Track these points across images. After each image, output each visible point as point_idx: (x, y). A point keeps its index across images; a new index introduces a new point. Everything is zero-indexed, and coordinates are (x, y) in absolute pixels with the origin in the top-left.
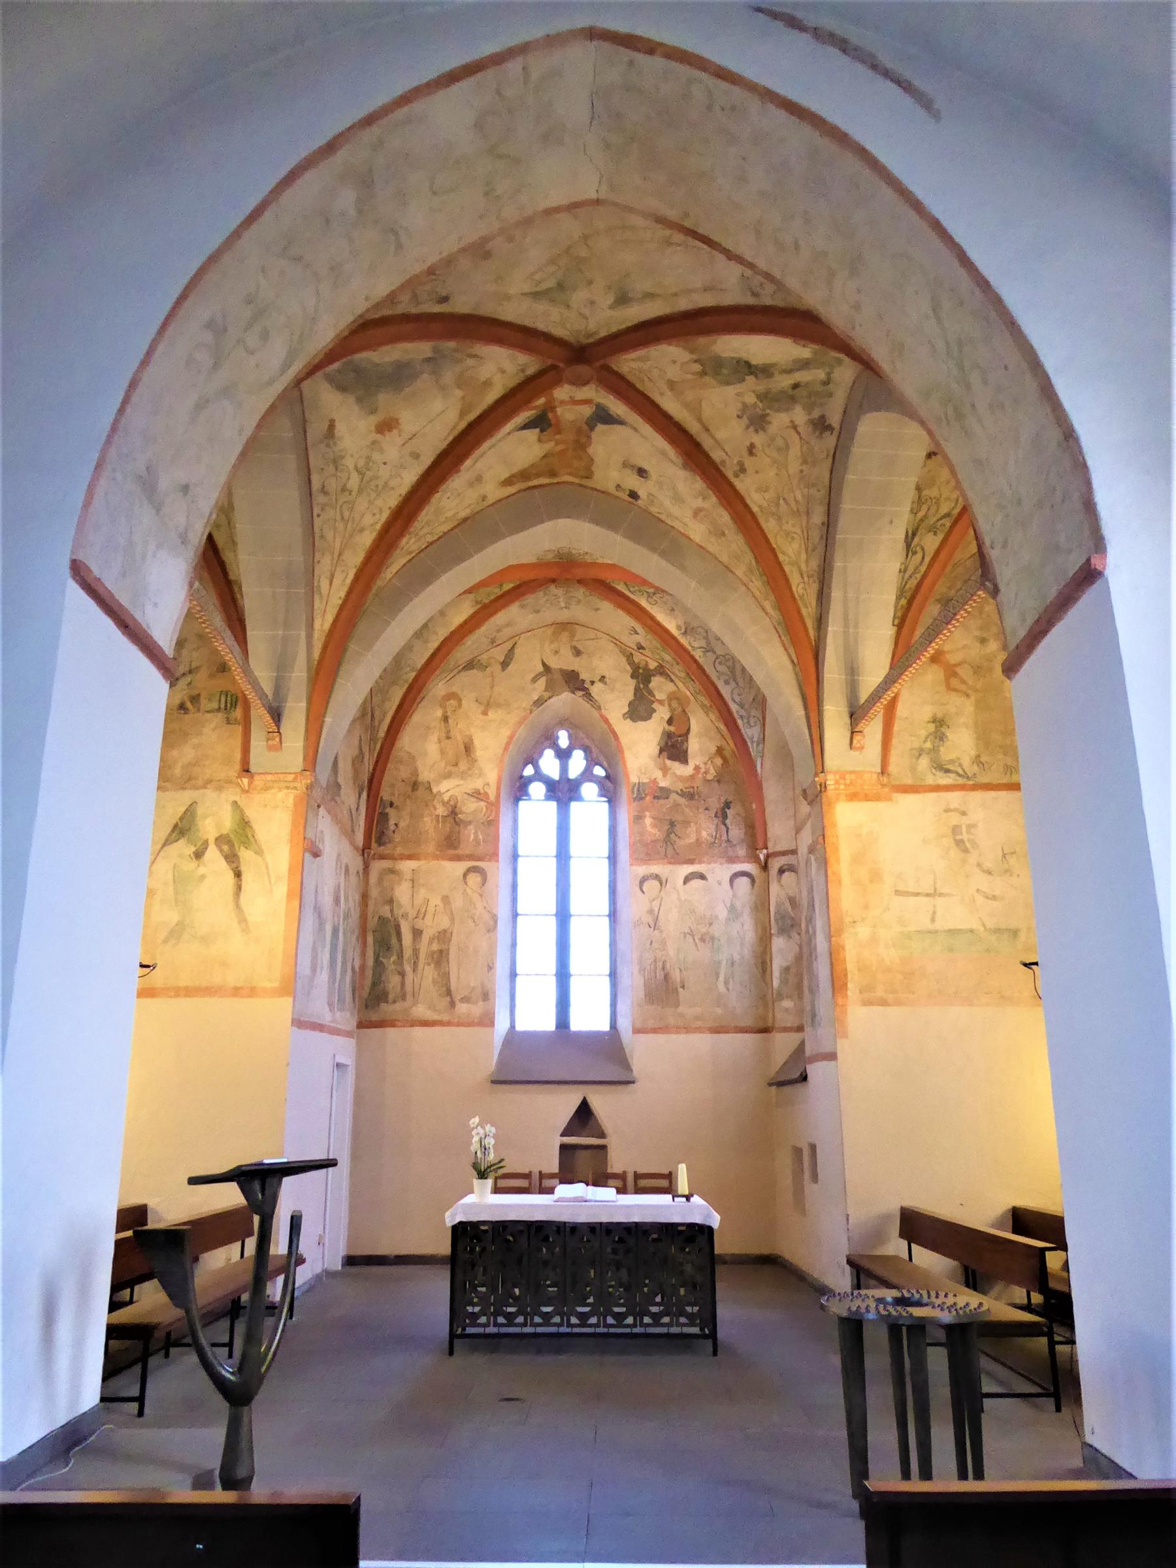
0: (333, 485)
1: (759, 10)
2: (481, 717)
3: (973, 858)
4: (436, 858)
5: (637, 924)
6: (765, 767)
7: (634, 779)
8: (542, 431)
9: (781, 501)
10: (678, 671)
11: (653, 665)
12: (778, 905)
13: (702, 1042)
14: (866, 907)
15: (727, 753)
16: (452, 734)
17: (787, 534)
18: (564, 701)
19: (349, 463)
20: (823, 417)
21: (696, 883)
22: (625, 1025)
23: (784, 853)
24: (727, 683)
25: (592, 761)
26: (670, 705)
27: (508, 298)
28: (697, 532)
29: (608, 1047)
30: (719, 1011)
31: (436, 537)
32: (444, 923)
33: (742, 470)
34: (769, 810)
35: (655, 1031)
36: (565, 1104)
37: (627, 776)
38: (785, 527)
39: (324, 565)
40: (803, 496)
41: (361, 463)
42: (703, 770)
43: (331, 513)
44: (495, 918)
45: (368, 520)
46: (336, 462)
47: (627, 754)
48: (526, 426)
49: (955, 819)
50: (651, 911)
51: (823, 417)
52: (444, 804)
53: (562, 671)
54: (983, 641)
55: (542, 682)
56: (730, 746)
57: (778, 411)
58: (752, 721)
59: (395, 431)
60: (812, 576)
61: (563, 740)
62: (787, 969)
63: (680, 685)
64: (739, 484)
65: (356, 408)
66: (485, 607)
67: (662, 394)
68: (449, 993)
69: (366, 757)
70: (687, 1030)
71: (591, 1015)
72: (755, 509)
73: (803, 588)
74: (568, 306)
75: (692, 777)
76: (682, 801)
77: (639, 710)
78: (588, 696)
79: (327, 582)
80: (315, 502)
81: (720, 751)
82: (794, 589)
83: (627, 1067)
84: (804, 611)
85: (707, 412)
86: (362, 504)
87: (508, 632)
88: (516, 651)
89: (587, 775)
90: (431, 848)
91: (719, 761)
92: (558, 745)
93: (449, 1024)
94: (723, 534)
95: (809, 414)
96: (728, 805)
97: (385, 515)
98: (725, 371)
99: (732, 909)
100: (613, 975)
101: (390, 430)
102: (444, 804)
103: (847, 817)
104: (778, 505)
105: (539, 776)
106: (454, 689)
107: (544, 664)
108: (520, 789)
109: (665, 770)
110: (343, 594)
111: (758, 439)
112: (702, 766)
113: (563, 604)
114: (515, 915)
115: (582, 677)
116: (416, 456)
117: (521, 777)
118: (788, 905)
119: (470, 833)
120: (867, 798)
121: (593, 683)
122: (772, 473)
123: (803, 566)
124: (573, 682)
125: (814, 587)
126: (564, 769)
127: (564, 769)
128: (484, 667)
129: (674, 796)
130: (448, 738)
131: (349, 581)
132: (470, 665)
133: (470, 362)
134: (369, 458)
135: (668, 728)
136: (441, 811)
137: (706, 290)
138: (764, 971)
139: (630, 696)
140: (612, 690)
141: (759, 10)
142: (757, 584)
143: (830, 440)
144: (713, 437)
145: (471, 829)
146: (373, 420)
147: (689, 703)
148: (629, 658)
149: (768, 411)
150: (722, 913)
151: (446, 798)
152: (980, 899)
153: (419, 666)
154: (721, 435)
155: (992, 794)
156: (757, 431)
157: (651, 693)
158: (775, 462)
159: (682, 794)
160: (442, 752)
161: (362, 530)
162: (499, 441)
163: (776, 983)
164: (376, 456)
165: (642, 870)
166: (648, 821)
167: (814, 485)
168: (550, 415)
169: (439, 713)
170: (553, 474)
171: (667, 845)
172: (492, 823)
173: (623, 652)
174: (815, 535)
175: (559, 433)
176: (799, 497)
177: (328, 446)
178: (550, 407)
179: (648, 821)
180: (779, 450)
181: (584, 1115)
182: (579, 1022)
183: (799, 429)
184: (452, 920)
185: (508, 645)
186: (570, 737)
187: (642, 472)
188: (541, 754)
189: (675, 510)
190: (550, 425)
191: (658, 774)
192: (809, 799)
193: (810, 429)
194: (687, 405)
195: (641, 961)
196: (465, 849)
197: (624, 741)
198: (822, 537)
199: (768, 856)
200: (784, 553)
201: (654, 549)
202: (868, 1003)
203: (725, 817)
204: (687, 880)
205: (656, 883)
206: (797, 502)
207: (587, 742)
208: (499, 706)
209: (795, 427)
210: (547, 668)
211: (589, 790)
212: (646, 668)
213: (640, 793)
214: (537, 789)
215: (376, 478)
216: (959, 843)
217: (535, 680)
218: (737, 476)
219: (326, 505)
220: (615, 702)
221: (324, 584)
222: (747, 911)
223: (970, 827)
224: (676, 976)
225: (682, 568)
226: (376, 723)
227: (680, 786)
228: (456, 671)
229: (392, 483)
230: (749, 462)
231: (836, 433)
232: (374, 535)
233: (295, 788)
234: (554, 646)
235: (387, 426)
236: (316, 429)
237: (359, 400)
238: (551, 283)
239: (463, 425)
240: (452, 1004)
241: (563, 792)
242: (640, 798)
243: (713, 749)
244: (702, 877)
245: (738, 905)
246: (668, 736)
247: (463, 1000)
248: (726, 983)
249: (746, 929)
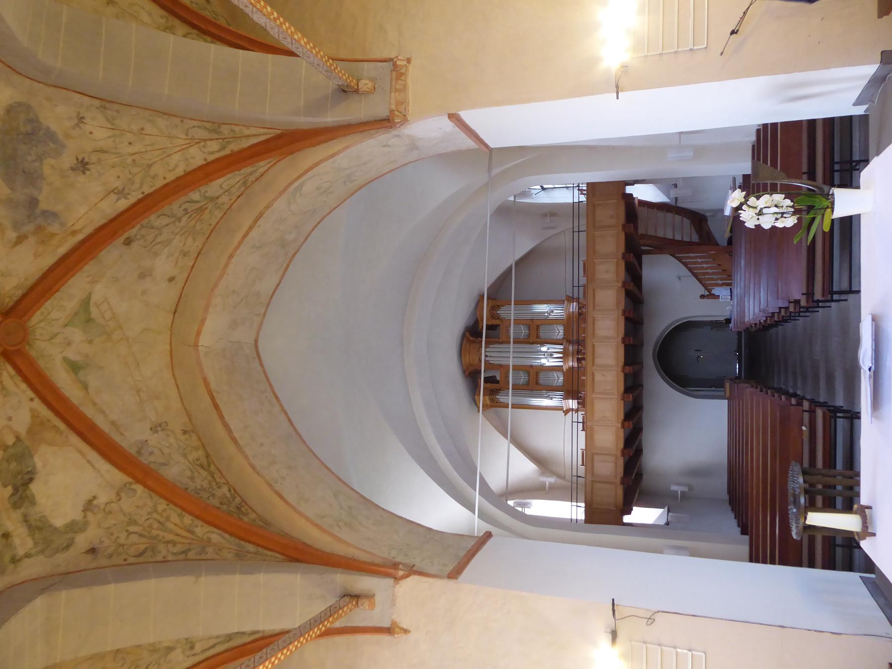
27: (93, 282)
74: (66, 326)
98: (13, 465)
133: (12, 235)
137: (113, 423)
238: (94, 312)
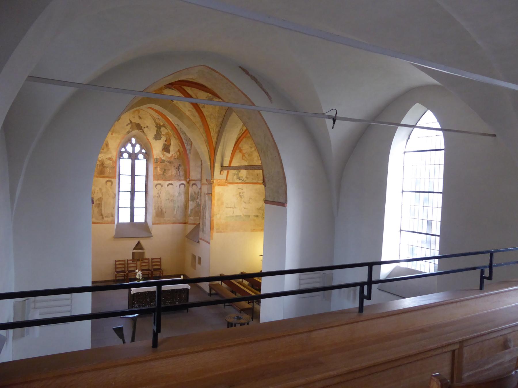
1: (240, 67)
3: (243, 200)
4: (97, 177)
5: (154, 197)
6: (191, 157)
7: (155, 157)
10: (169, 127)
11: (162, 124)
12: (191, 193)
13: (170, 227)
14: (219, 211)
15: (181, 151)
18: (136, 132)
21: (170, 186)
22: (150, 222)
23: (194, 180)
25: (142, 148)
28: (188, 113)
29: (144, 226)
30: (174, 219)
32: (100, 196)
33: (204, 107)
34: (191, 168)
35: (158, 224)
36: (133, 243)
37: (153, 156)
44: (115, 194)
47: (154, 150)
49: (240, 191)
50: (158, 193)
52: (100, 161)
54: (251, 148)
55: (130, 126)
56: (182, 149)
61: (134, 141)
62: (192, 210)
68: (102, 215)
70: (166, 224)
71: (139, 218)
73: (214, 135)
75: (171, 157)
76: (168, 164)
77: (157, 137)
78: (143, 131)
81: (179, 151)
83: (150, 233)
84: (213, 140)
89: (141, 152)
90: (96, 174)
91: (178, 153)
93: (102, 223)
96: (180, 165)
99: (179, 193)
100: (146, 208)
102: (100, 161)
103: (217, 190)
105: (126, 151)
108: (121, 155)
109: (164, 155)
114: (119, 191)
115: (141, 125)
117: (121, 152)
118: (194, 194)
119: (108, 170)
120: (222, 185)
124: (138, 127)
125: (216, 135)
126: (134, 150)
127: (134, 150)
129: (166, 162)
136: (98, 163)
138: (186, 209)
141: (240, 67)
142: (202, 130)
145: (108, 169)
148: (155, 121)
150: (177, 194)
151: (100, 159)
152: (243, 209)
155: (248, 185)
157: (161, 132)
159: (168, 162)
163: (189, 213)
165: (156, 182)
166: (158, 169)
171: (163, 176)
172: (114, 168)
179: (158, 169)
181: (139, 246)
182: (136, 221)
184: (103, 195)
188: (127, 145)
191: (162, 156)
195: (155, 206)
196: (106, 175)
197: (153, 146)
199: (189, 181)
201: (176, 116)
202: (218, 232)
203: (179, 169)
204: (168, 185)
205: (160, 186)
207: (141, 143)
210: (131, 122)
211: (141, 156)
212: (160, 125)
213: (156, 161)
214: (126, 155)
216: (240, 196)
217: (127, 125)
220: (150, 134)
222: (183, 193)
223: (243, 192)
224: (164, 210)
225: (183, 122)
227: (167, 160)
240: (103, 218)
241: (133, 157)
242: (156, 162)
244: (172, 184)
245: (181, 192)
246: (165, 145)
247: (106, 217)
248: (176, 212)
249: (182, 198)
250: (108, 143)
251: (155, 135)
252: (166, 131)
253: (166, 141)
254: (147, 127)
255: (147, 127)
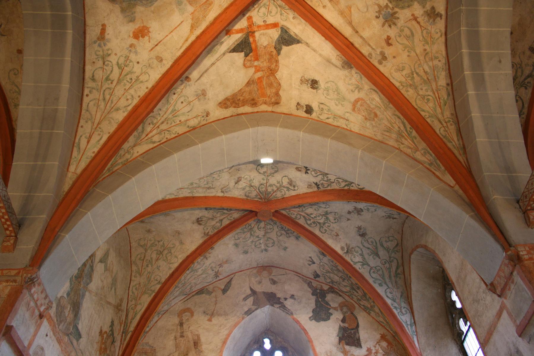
0: (99, 74)
2: (208, 322)
8: (246, 55)
9: (415, 75)
16: (185, 334)
17: (423, 97)
19: (113, 59)
20: (433, 8)
24: (380, 285)
26: (341, 310)
31: (173, 136)
38: (421, 93)
39: (85, 128)
40: (430, 67)
41: (122, 61)
42: (374, 351)
43: (95, 95)
45: (122, 103)
46: (104, 58)
47: (315, 343)
48: (236, 49)
51: (433, 8)
53: (264, 293)
55: (252, 299)
57: (403, 8)
58: (403, 310)
59: (146, 38)
60: (449, 121)
61: (267, 345)
63: (347, 298)
64: (381, 68)
65: (121, 16)
66: (211, 237)
67: (324, 7)
69: (117, 344)
72: (397, 84)
77: (321, 313)
78: (283, 307)
79: (86, 140)
80: (86, 85)
81: (383, 337)
82: (438, 132)
84: (449, 145)
85: (356, 17)
86: (119, 91)
87: (226, 270)
88: (233, 282)
91: (384, 344)
92: (263, 347)
94: (376, 115)
95: (424, 7)
97: (136, 101)
101: (143, 37)
104: (413, 78)
106: (189, 306)
107: (251, 289)
110: (96, 150)
111: (392, 32)
112: (373, 348)
113: (263, 247)
115: (278, 295)
116: (160, 60)
121: (286, 299)
122: (405, 55)
123: (440, 116)
125: (452, 128)
128: (209, 293)
130: (182, 336)
131: (102, 142)
132: (200, 292)
134: (127, 58)
135: (342, 324)
139: (313, 305)
140: (300, 303)
143: (441, 24)
144: (361, 37)
146: (132, 27)
147: (354, 308)
148: (310, 284)
149: (396, 9)
153: (163, 280)
154: (366, 34)
156: (390, 26)
157: (327, 303)
158: (406, 47)
160: (177, 346)
161: (118, 109)
162: (218, 60)
164: (133, 57)
167: (436, 58)
168: (251, 40)
169: (176, 320)
170: (254, 103)
173: (305, 281)
174: (444, 94)
175: (257, 59)
176: (427, 68)
177: (100, 46)
178: (250, 33)
180: (407, 37)
183: (418, 20)
185: (227, 280)
186: (271, 343)
187: (314, 84)
189: (339, 110)
190: (251, 50)
192: (498, 291)
193: (426, 18)
194: (342, 13)
197: (312, 334)
198: (448, 95)
200: (423, 111)
206: (426, 72)
208: (219, 315)
209: (415, 19)
210: (254, 292)
212: (322, 290)
215: (131, 72)
217: (245, 299)
218: (380, 63)
219: (93, 88)
221: (84, 142)
226: (129, 320)
228: (191, 295)
229: (143, 78)
230: (389, 51)
231: (444, 17)
232: (125, 114)
233: (15, 281)
234: (258, 279)
235: (141, 33)
236: (92, 33)
237: (123, 10)
239: (193, 38)
243: (379, 337)
250: (198, 336)
251: (313, 311)
252: (340, 300)
253: (343, 321)
254: (292, 296)
255: (292, 296)
